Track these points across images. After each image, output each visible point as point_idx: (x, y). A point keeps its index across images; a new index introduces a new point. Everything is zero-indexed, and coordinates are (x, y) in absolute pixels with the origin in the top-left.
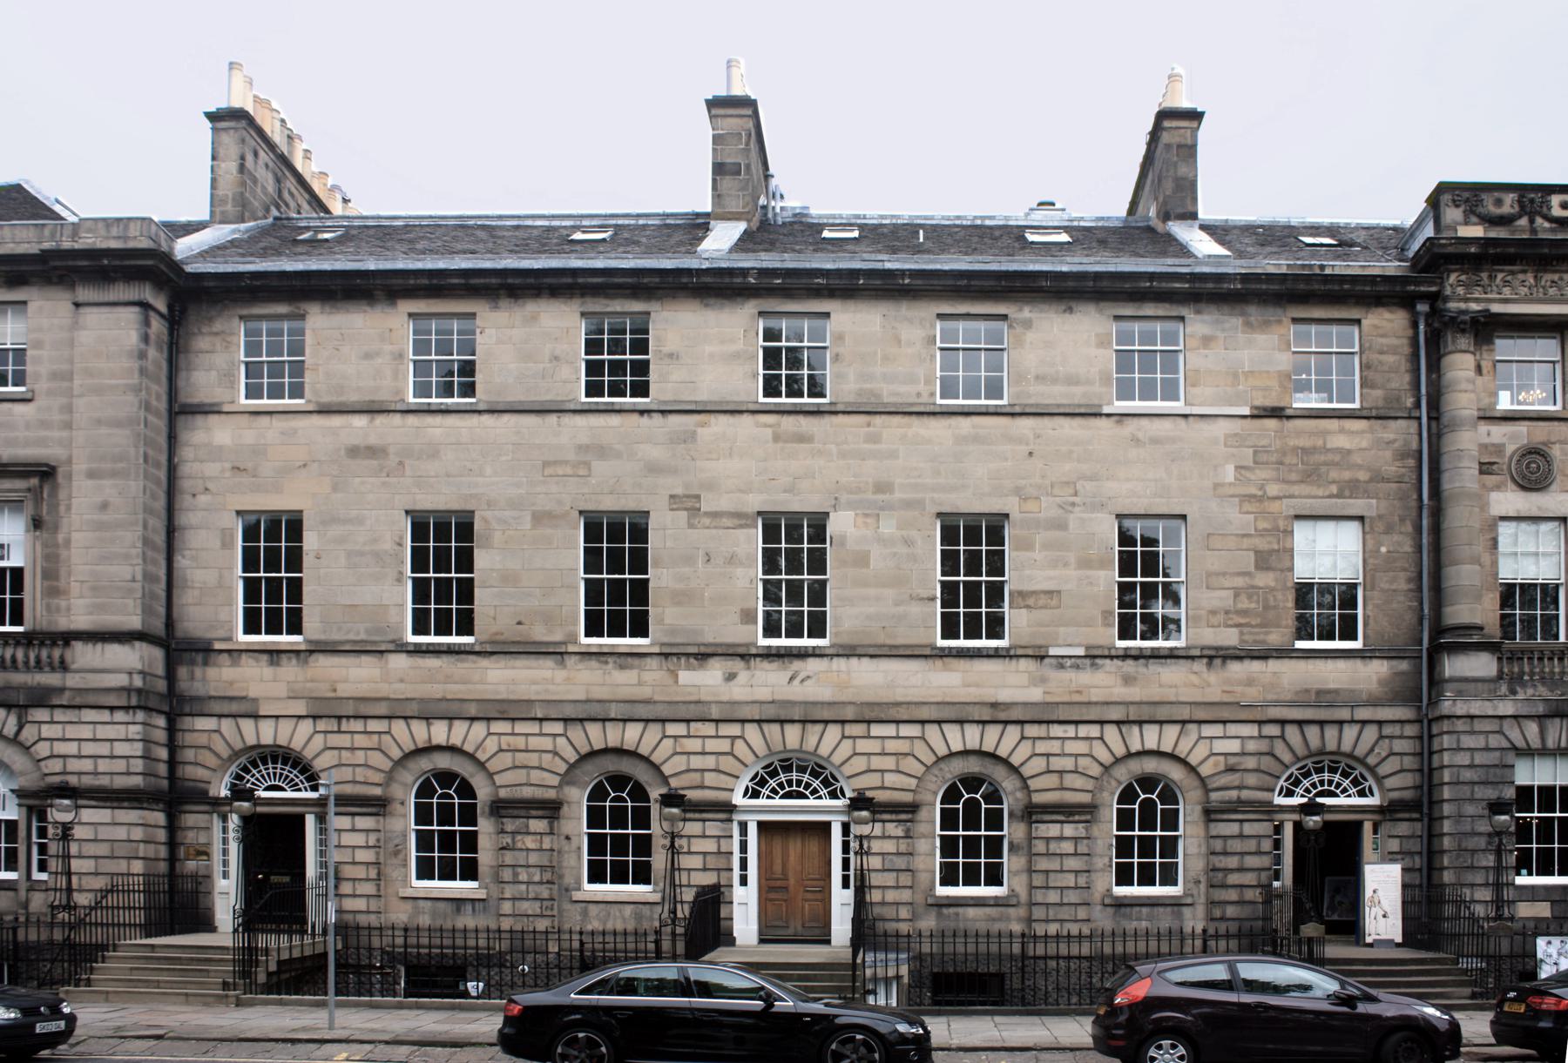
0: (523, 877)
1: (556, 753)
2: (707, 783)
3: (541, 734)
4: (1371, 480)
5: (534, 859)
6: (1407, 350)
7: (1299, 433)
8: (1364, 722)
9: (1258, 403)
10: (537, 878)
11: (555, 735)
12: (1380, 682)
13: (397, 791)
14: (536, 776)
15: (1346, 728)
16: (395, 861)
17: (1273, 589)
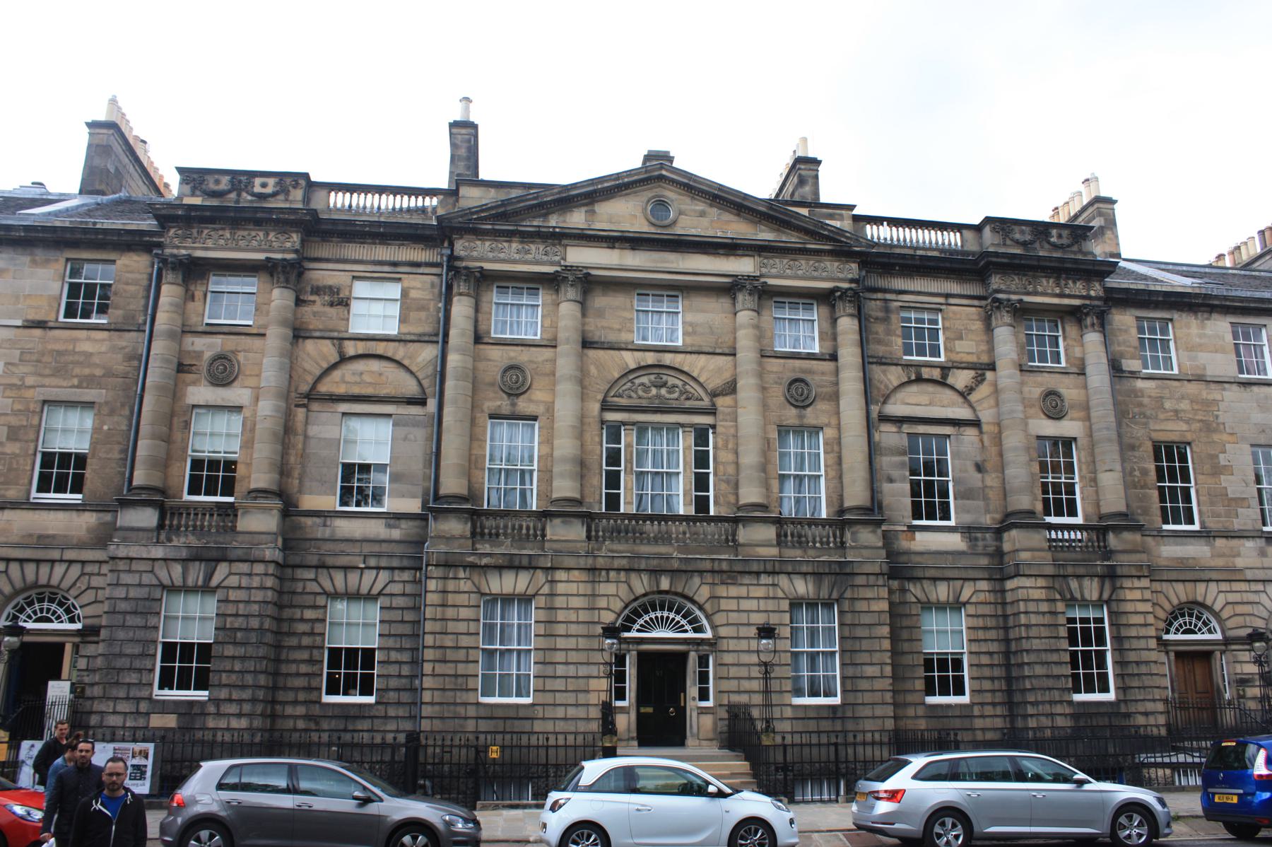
4: (104, 376)
6: (145, 283)
7: (57, 340)
8: (71, 562)
9: (30, 317)
12: (89, 530)
15: (57, 566)
17: (16, 456)
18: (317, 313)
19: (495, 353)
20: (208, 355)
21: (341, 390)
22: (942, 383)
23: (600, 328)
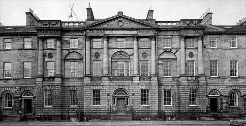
18: (65, 46)
19: (94, 51)
20: (48, 53)
21: (69, 58)
22: (170, 52)
23: (111, 45)
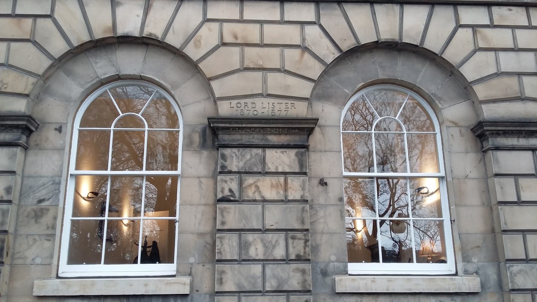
0: (257, 250)
1: (305, 49)
2: (528, 93)
3: (283, 22)
5: (274, 217)
10: (279, 253)
11: (303, 23)
13: (52, 110)
14: (277, 83)
16: (35, 229)
